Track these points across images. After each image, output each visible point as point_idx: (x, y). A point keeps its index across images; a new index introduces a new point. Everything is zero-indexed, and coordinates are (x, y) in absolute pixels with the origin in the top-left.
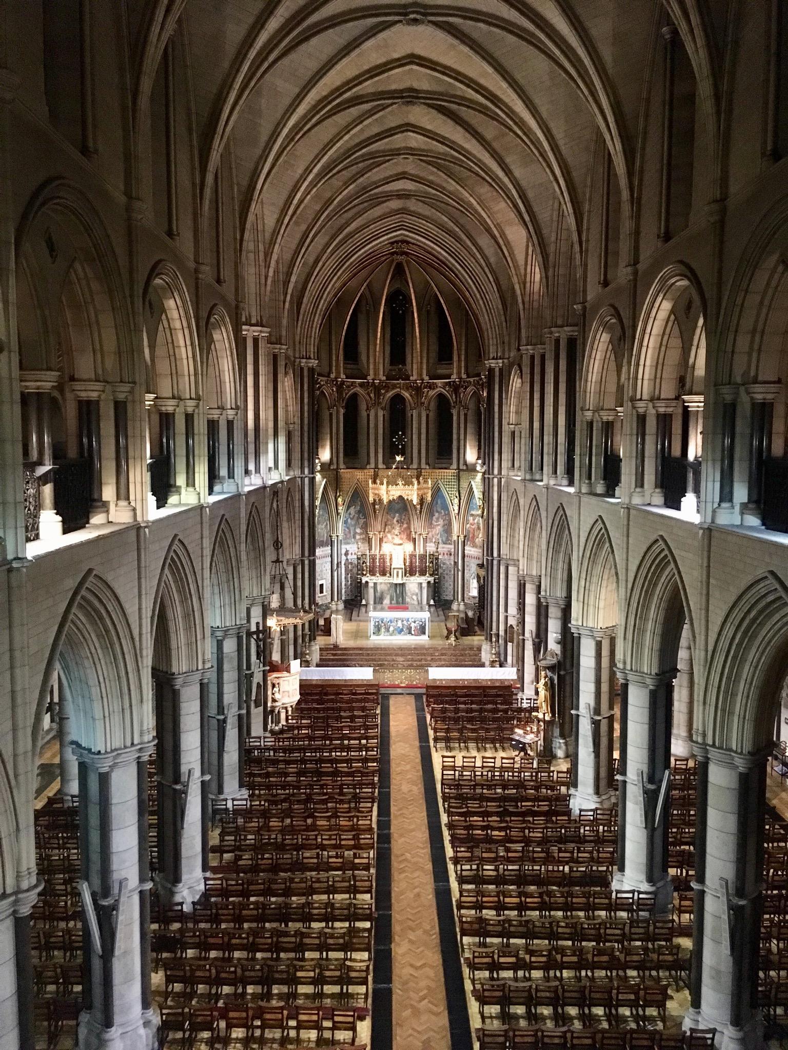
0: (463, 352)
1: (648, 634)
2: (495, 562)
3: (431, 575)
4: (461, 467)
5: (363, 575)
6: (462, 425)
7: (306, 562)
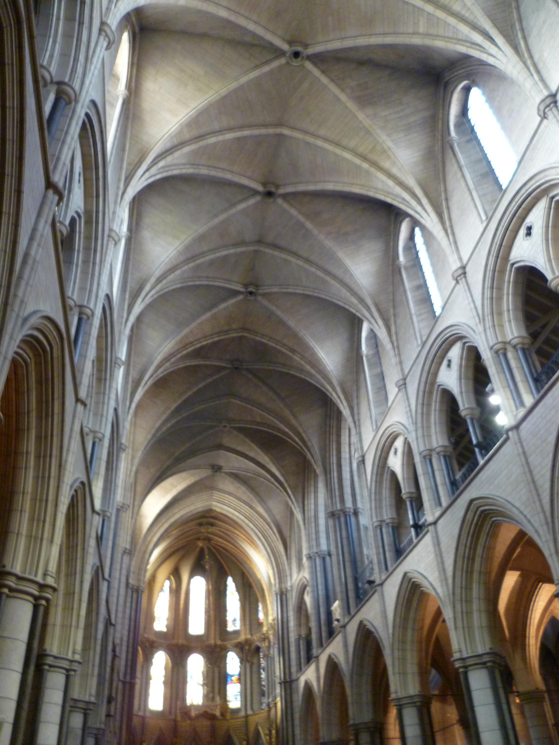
1: (475, 616)
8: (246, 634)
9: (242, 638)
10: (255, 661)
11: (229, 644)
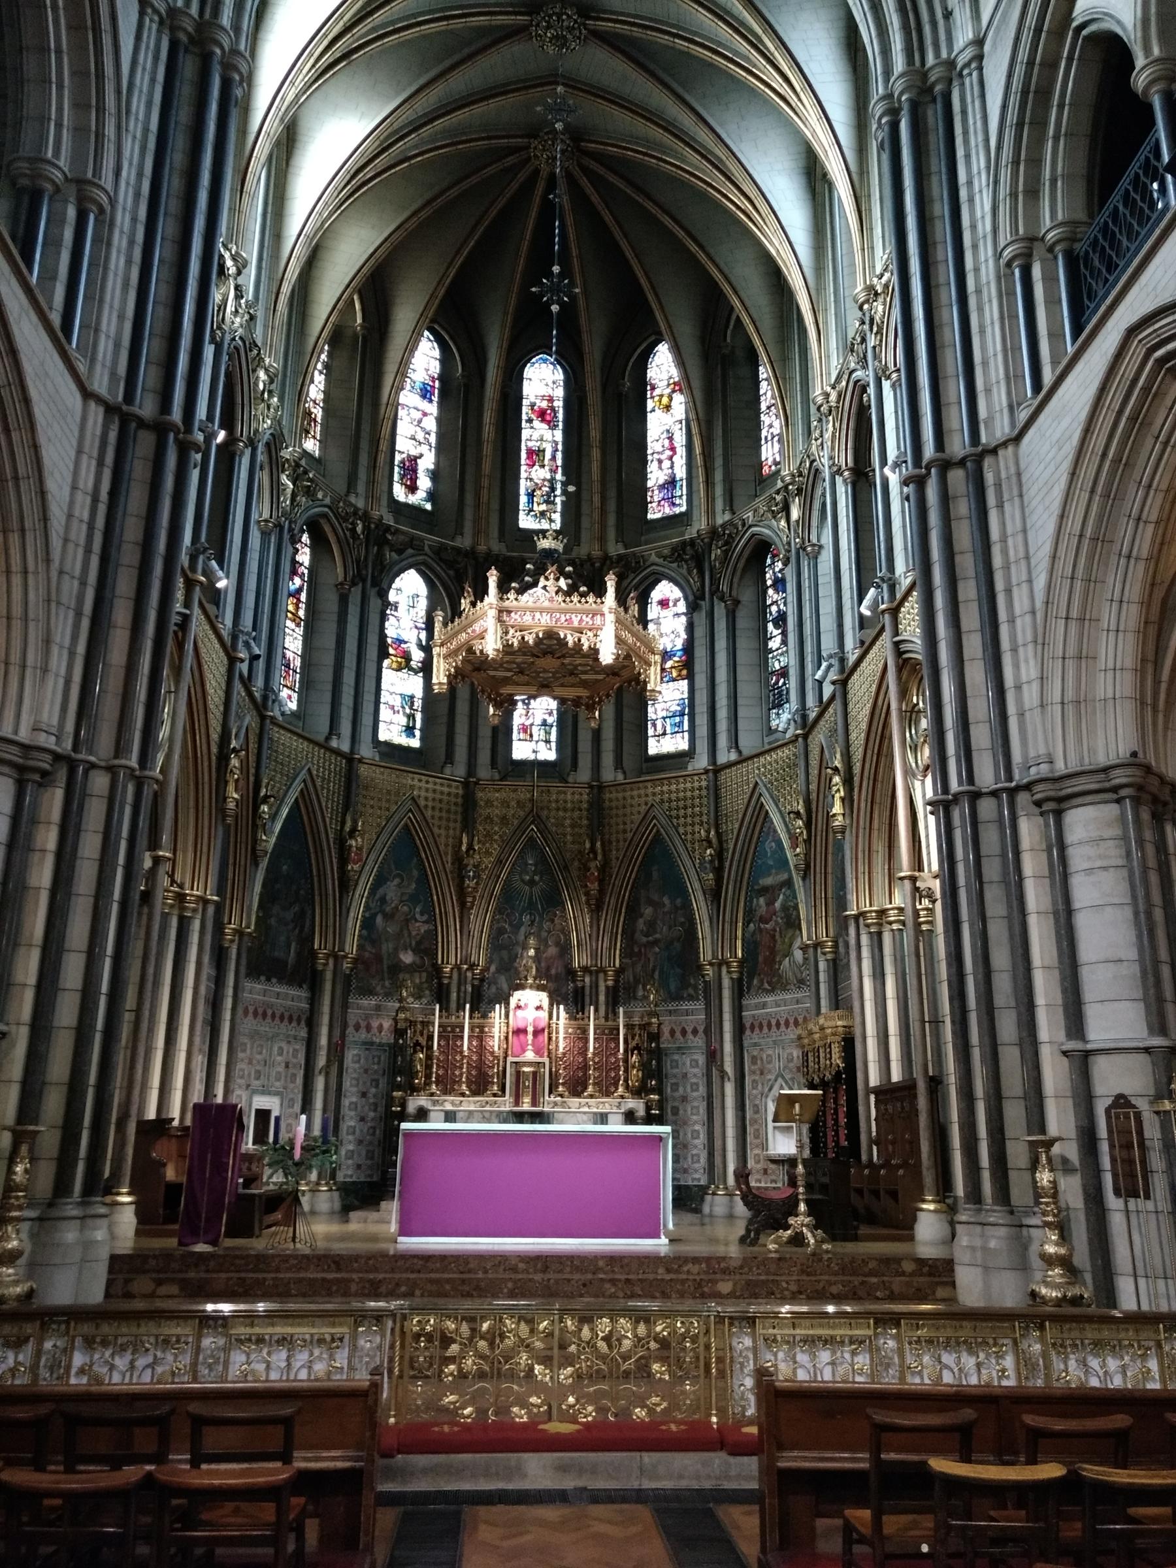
0: (719, 462)
2: (987, 807)
3: (637, 1093)
4: (723, 757)
5: (414, 1090)
6: (721, 644)
7: (100, 782)
8: (711, 512)
9: (700, 524)
10: (747, 596)
11: (652, 552)
